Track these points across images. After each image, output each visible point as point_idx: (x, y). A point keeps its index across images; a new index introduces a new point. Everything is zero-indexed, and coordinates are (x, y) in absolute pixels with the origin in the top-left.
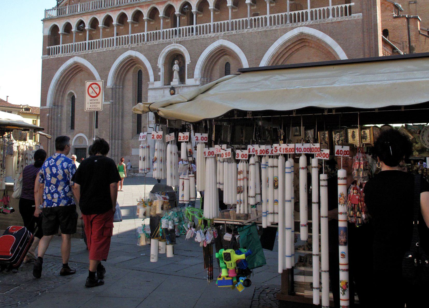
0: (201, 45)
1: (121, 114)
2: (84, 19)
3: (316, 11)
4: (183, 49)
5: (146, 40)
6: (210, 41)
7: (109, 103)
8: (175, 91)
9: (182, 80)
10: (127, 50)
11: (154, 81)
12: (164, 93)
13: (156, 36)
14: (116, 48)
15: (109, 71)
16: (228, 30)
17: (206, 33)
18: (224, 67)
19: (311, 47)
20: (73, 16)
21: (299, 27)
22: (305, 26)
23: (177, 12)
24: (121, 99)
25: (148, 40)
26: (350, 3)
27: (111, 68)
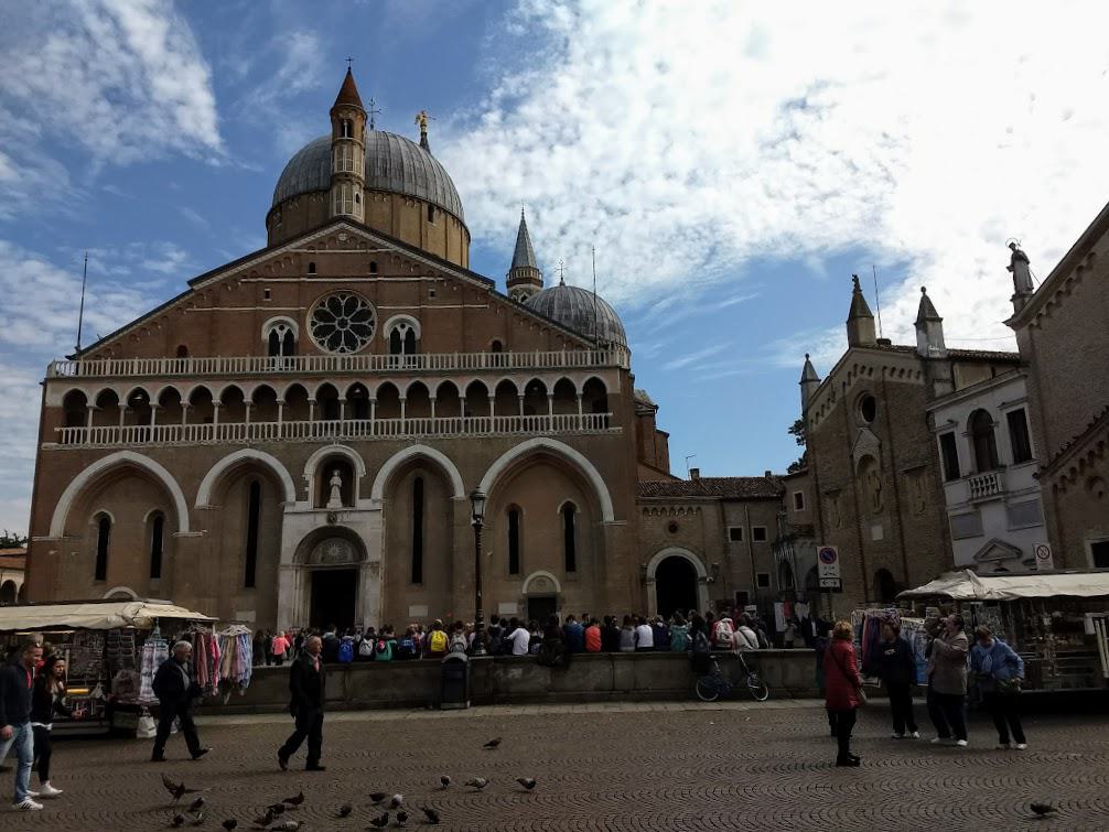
4: (351, 453)
7: (201, 534)
9: (347, 499)
10: (243, 447)
11: (297, 500)
12: (315, 519)
13: (298, 432)
17: (393, 433)
23: (342, 396)
25: (283, 435)
26: (606, 411)
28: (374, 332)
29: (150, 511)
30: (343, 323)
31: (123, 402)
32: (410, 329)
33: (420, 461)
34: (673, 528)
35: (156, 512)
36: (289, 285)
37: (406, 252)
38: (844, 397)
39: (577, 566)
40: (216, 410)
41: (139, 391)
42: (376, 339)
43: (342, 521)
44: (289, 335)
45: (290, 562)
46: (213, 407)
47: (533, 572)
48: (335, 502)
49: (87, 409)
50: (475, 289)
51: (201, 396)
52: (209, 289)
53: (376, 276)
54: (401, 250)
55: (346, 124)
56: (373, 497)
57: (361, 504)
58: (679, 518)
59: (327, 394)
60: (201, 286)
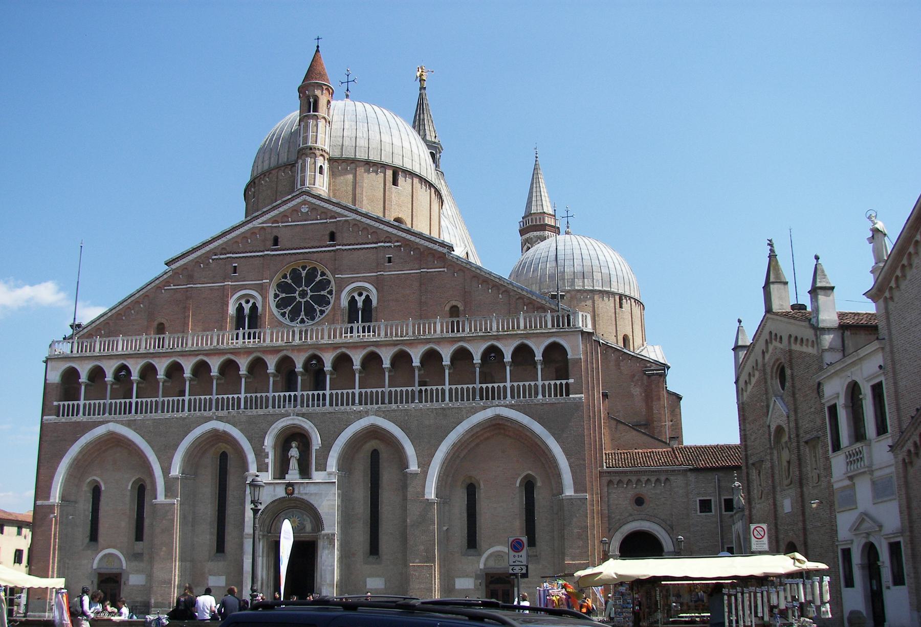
0: (339, 422)
2: (129, 364)
3: (519, 386)
4: (307, 425)
5: (242, 406)
6: (355, 417)
8: (294, 489)
9: (305, 472)
10: (209, 419)
12: (274, 490)
14: (189, 415)
15: (176, 450)
16: (383, 403)
18: (370, 457)
19: (507, 436)
20: (110, 357)
21: (494, 406)
22: (502, 406)
23: (299, 368)
25: (246, 408)
27: (178, 446)
28: (332, 302)
29: (134, 479)
30: (303, 294)
31: (109, 378)
32: (367, 297)
33: (374, 432)
34: (639, 501)
35: (139, 479)
37: (364, 220)
38: (764, 365)
39: (537, 543)
40: (187, 383)
41: (124, 367)
42: (333, 308)
43: (299, 493)
44: (254, 308)
47: (491, 546)
48: (293, 476)
49: (80, 384)
50: (433, 253)
51: (175, 370)
52: (184, 268)
54: (359, 218)
55: (312, 100)
56: (328, 470)
58: (647, 491)
59: (286, 364)
60: (177, 265)
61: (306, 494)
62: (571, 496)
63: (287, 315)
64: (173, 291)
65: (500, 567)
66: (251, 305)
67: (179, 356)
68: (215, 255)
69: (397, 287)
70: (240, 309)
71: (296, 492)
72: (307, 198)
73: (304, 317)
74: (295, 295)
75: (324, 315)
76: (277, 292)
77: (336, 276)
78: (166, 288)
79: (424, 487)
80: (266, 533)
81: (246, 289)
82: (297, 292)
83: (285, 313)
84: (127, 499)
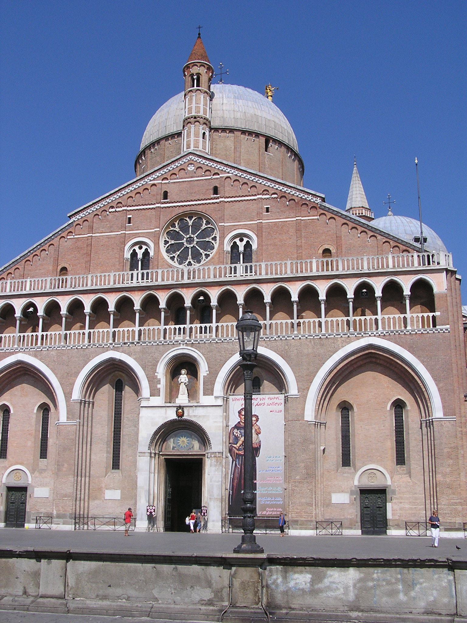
0: (224, 352)
1: (89, 439)
10: (108, 349)
11: (151, 396)
12: (166, 413)
19: (378, 364)
23: (188, 303)
24: (90, 418)
27: (79, 373)
28: (216, 246)
30: (190, 240)
31: (18, 314)
36: (147, 211)
44: (146, 253)
45: (146, 449)
46: (86, 316)
48: (182, 399)
53: (218, 198)
55: (195, 77)
57: (205, 400)
61: (195, 416)
62: (441, 418)
63: (175, 259)
64: (74, 240)
65: (372, 484)
66: (144, 251)
67: (80, 294)
68: (112, 208)
69: (275, 233)
70: (134, 254)
71: (185, 414)
72: (193, 157)
73: (191, 260)
74: (183, 241)
75: (209, 258)
76: (167, 240)
77: (220, 224)
78: (68, 237)
79: (303, 409)
80: (157, 452)
81: (139, 237)
82: (185, 239)
83: (174, 257)
84: (33, 421)
